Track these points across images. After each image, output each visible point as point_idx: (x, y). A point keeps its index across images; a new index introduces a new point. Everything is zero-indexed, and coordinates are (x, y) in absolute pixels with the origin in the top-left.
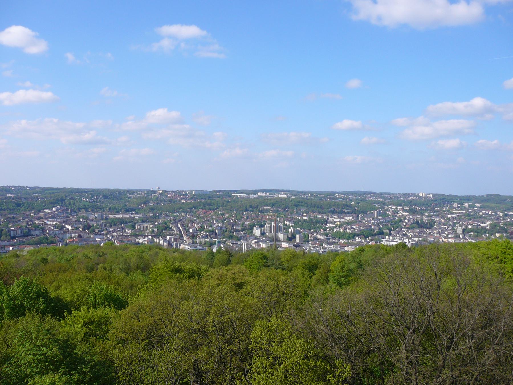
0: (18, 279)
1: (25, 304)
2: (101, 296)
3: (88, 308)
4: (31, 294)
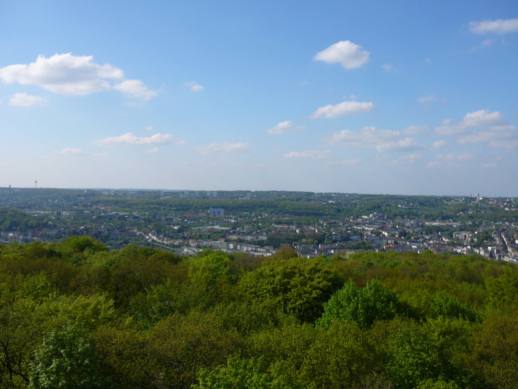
0: (370, 283)
1: (377, 306)
2: (447, 306)
3: (444, 318)
4: (382, 298)
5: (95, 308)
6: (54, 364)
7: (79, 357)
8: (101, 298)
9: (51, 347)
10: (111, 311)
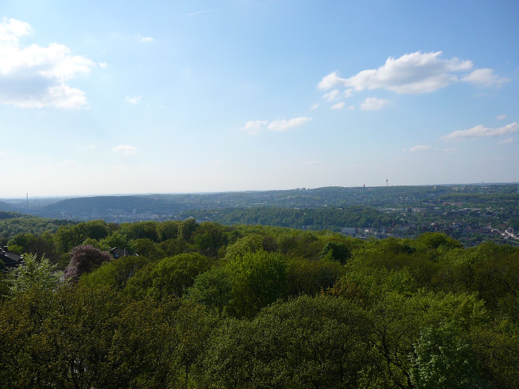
5: (465, 306)
6: (433, 359)
7: (458, 356)
8: (472, 297)
9: (429, 342)
10: (482, 312)
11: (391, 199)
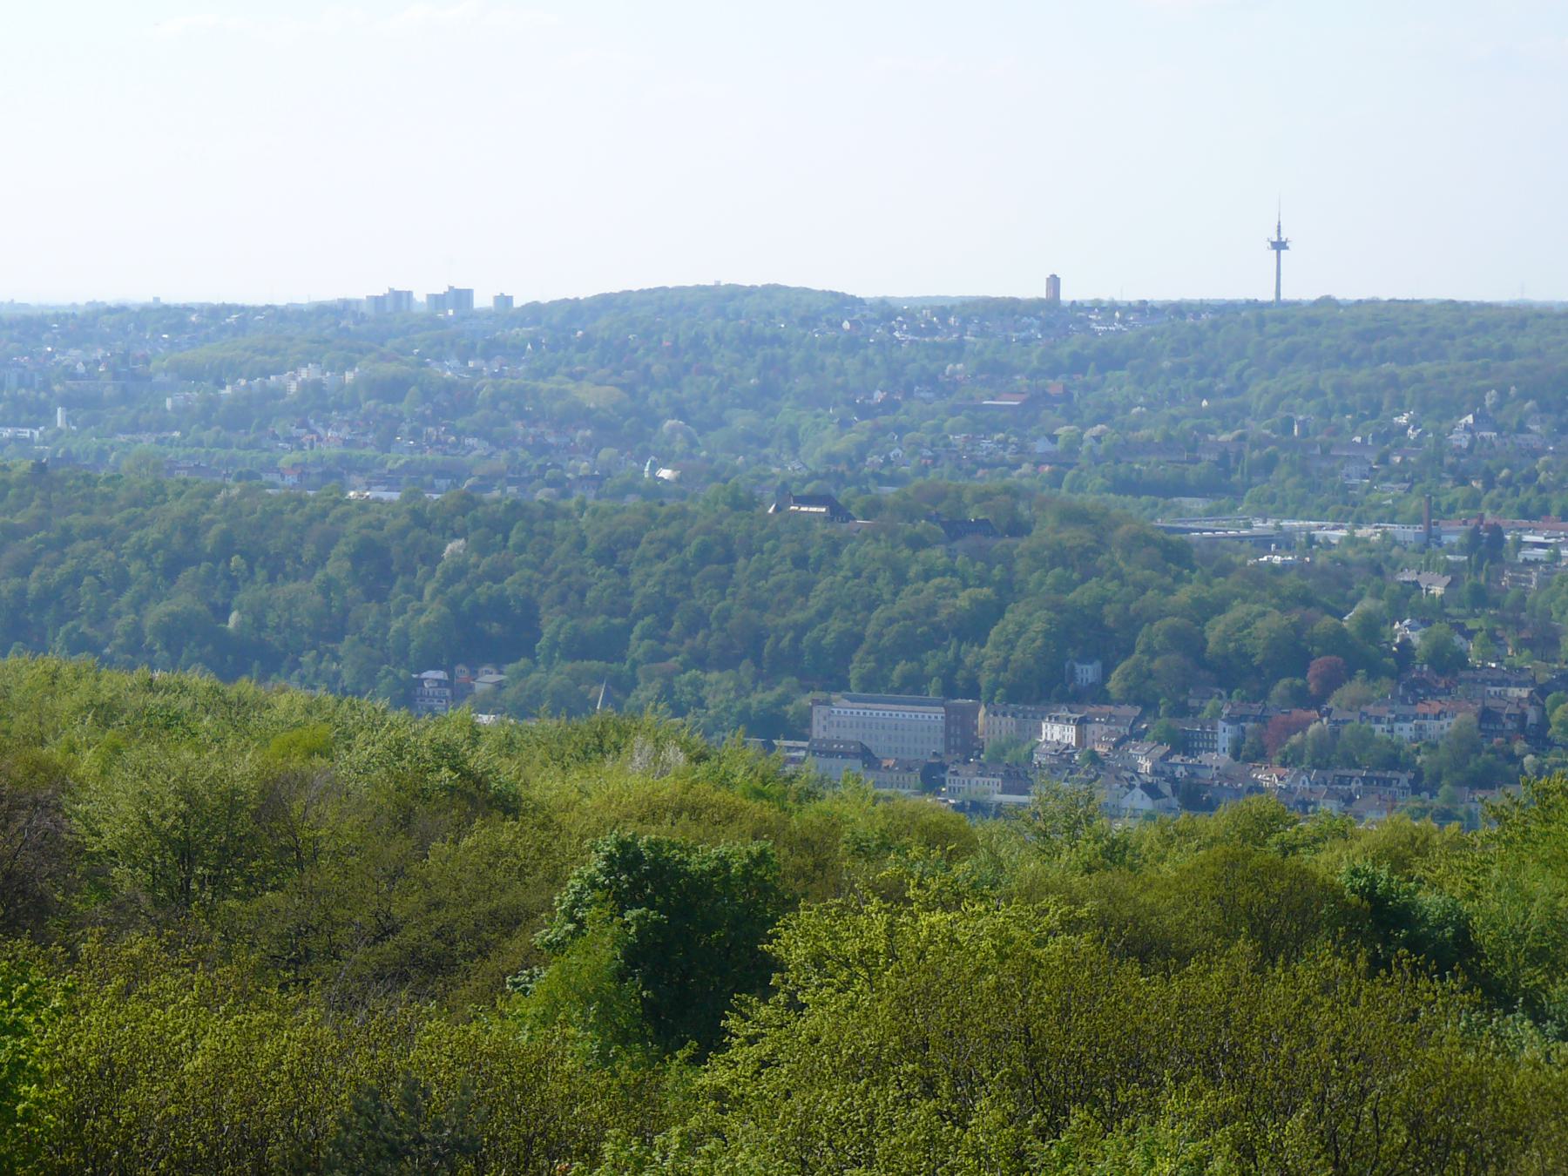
11: (1305, 432)
